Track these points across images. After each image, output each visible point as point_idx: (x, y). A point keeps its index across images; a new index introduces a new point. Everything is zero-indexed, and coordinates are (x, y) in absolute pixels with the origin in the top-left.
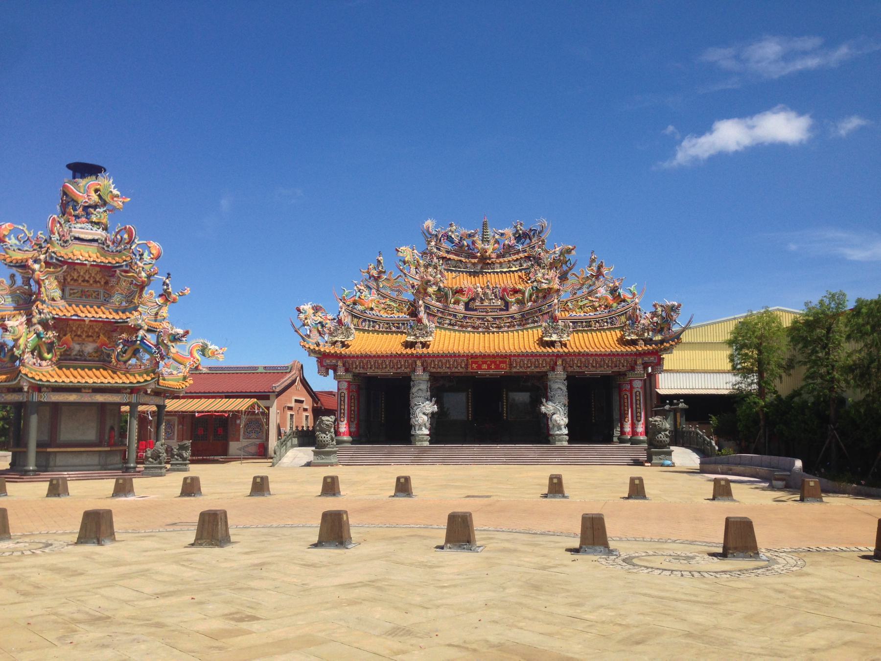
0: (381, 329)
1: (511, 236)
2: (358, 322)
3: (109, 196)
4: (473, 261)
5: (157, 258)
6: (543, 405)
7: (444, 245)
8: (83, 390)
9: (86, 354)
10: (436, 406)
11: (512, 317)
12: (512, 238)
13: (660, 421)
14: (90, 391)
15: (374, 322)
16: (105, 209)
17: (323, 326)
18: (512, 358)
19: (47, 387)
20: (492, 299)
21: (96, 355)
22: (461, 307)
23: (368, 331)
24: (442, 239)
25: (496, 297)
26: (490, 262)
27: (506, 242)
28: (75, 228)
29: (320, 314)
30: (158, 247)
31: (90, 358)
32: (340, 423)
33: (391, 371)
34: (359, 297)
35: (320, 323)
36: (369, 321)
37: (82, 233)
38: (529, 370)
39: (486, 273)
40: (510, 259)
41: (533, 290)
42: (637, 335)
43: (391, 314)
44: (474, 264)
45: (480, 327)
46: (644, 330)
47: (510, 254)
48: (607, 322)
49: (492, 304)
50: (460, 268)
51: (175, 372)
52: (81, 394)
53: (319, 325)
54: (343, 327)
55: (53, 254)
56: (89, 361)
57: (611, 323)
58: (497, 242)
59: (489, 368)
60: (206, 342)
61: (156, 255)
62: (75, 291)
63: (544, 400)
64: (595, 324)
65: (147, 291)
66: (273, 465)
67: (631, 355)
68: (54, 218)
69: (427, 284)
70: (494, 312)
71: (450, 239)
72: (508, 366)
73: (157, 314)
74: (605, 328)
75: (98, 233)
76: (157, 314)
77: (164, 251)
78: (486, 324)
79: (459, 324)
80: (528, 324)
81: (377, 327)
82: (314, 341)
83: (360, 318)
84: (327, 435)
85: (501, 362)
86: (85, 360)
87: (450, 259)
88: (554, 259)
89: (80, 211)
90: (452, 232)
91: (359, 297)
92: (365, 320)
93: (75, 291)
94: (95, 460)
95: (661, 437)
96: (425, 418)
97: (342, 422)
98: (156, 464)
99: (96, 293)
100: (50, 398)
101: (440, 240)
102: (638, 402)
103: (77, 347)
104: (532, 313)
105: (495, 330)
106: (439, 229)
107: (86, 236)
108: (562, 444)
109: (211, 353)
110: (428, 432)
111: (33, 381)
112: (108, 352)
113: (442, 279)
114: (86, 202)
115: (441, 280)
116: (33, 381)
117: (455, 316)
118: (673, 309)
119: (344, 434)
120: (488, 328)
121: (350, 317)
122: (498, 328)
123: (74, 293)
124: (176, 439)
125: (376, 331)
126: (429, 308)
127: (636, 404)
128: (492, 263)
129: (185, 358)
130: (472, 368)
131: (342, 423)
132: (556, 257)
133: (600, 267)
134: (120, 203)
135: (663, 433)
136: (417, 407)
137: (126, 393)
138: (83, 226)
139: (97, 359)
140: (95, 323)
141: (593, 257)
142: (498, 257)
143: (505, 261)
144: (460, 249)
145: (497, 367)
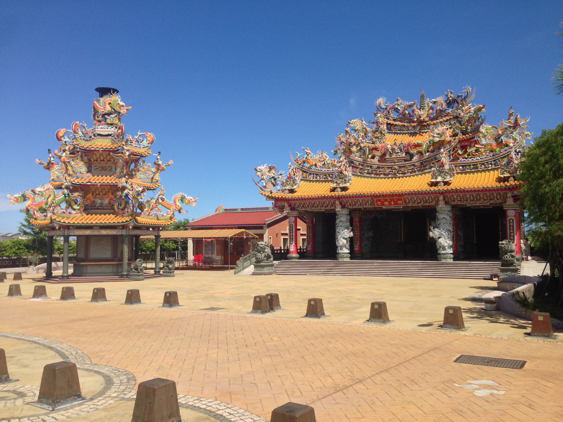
0: (321, 179)
1: (443, 102)
2: (306, 175)
3: (117, 107)
4: (413, 124)
5: (152, 143)
6: (431, 231)
7: (392, 115)
8: (94, 228)
9: (104, 205)
10: (352, 233)
11: (413, 165)
12: (444, 104)
13: (506, 244)
14: (98, 228)
15: (316, 175)
16: (115, 115)
17: (275, 179)
18: (405, 196)
19: (73, 226)
20: (398, 153)
21: (109, 206)
22: (376, 160)
23: (313, 181)
24: (390, 111)
25: (401, 150)
26: (426, 124)
27: (438, 108)
28: (97, 128)
29: (273, 171)
30: (152, 136)
31: (106, 208)
32: (290, 245)
33: (322, 208)
34: (306, 158)
35: (273, 177)
36: (313, 174)
37: (102, 131)
38: (420, 205)
39: (423, 133)
40: (441, 120)
41: (430, 143)
42: (509, 172)
43: (328, 169)
44: (414, 127)
45: (390, 174)
46: (516, 170)
47: (442, 117)
48: (491, 164)
49: (398, 156)
50: (404, 131)
51: (165, 215)
52: (93, 230)
53: (272, 179)
54: (291, 180)
55: (77, 146)
56: (106, 209)
57: (495, 164)
58: (432, 108)
59: (390, 204)
60: (183, 194)
61: (150, 141)
62: (98, 167)
63: (432, 228)
64: (481, 166)
65: (147, 164)
66: (235, 273)
67: (501, 189)
68: (77, 124)
69: (350, 145)
70: (400, 162)
71: (396, 110)
72: (403, 202)
73: (152, 178)
74: (489, 168)
75: (111, 130)
76: (152, 178)
77: (156, 140)
78: (394, 172)
79: (375, 173)
80: (426, 169)
81: (318, 178)
82: (269, 190)
83: (307, 172)
84: (261, 254)
85: (398, 200)
86: (103, 209)
87: (396, 125)
88: (469, 117)
89: (100, 118)
90: (398, 105)
91: (306, 158)
92: (310, 174)
93: (98, 167)
94: (110, 269)
95: (507, 257)
96: (345, 241)
97: (291, 244)
98: (136, 273)
99: (110, 167)
100: (75, 233)
101: (389, 112)
102: (511, 228)
103: (99, 201)
104: (429, 161)
105: (400, 175)
106: (388, 104)
107: (104, 133)
108: (447, 261)
109: (187, 201)
110: (349, 252)
111: (60, 223)
112: (113, 203)
113: (363, 140)
114: (103, 112)
115: (362, 142)
116: (60, 223)
117: (371, 167)
119: (293, 252)
120: (395, 174)
121: (301, 172)
122: (403, 174)
123: (97, 169)
124: (216, 254)
125: (318, 181)
126: (353, 162)
127: (510, 229)
128: (428, 125)
129: (170, 205)
130: (378, 205)
131: (291, 245)
132: (471, 115)
133: (516, 120)
134: (125, 110)
135: (509, 254)
136: (339, 233)
137: (119, 229)
138: (102, 126)
139: (110, 208)
140: (105, 186)
141: (511, 112)
142: (432, 120)
143: (437, 123)
144: (404, 117)
145: (396, 203)
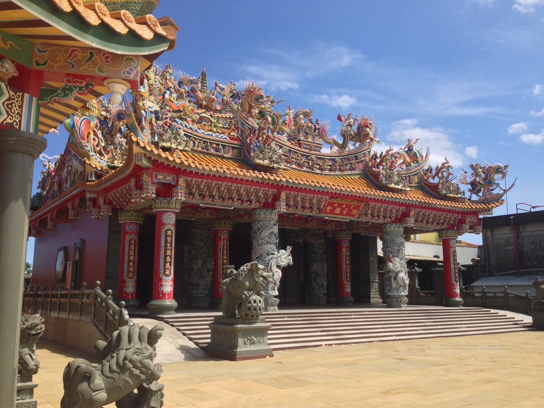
80: (346, 170)
97: (168, 276)
118: (498, 170)
120: (311, 168)
143: (222, 117)
